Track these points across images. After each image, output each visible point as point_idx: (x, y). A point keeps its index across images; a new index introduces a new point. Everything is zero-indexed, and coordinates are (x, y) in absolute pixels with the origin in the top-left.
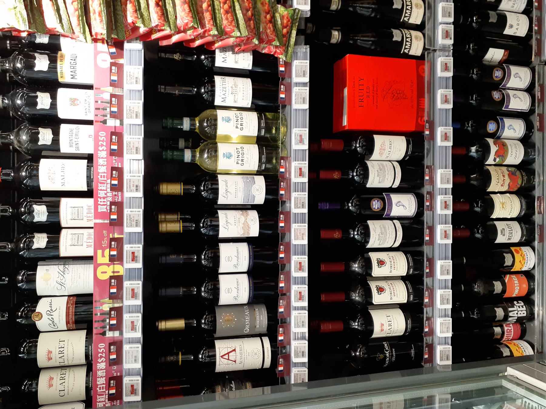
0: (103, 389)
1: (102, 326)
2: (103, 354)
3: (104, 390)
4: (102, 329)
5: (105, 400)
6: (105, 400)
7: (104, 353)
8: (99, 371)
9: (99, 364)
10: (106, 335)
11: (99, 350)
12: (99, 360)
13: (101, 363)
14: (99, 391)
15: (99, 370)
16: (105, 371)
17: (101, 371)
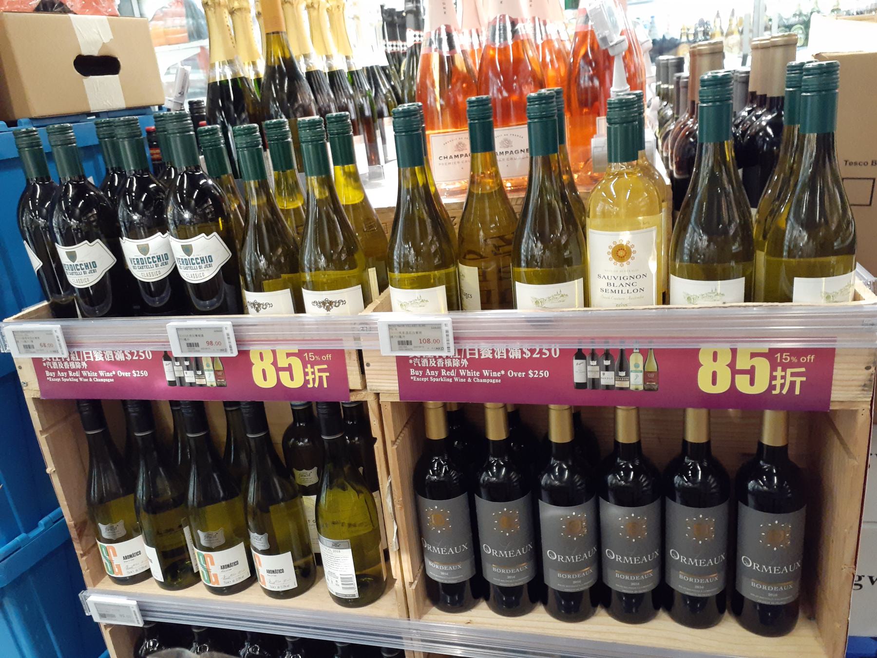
0: (470, 354)
3: (468, 357)
10: (576, 359)
16: (505, 357)
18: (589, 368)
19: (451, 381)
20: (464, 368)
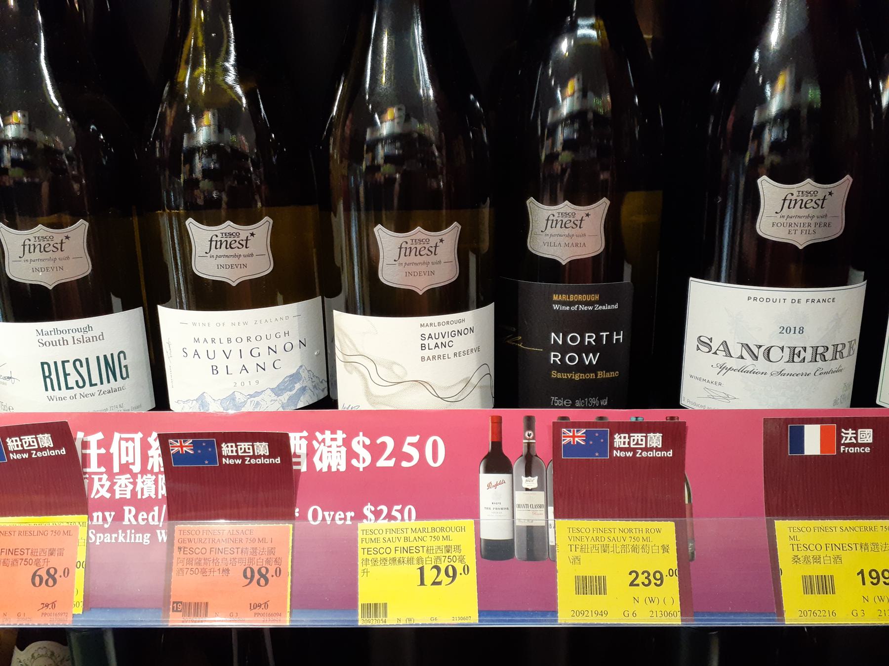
1: (537, 450)
2: (388, 458)
4: (524, 451)
5: (152, 472)
6: (152, 472)
7: (398, 463)
8: (304, 443)
10: (488, 470)
11: (415, 439)
12: (361, 438)
15: (310, 438)
18: (520, 497)
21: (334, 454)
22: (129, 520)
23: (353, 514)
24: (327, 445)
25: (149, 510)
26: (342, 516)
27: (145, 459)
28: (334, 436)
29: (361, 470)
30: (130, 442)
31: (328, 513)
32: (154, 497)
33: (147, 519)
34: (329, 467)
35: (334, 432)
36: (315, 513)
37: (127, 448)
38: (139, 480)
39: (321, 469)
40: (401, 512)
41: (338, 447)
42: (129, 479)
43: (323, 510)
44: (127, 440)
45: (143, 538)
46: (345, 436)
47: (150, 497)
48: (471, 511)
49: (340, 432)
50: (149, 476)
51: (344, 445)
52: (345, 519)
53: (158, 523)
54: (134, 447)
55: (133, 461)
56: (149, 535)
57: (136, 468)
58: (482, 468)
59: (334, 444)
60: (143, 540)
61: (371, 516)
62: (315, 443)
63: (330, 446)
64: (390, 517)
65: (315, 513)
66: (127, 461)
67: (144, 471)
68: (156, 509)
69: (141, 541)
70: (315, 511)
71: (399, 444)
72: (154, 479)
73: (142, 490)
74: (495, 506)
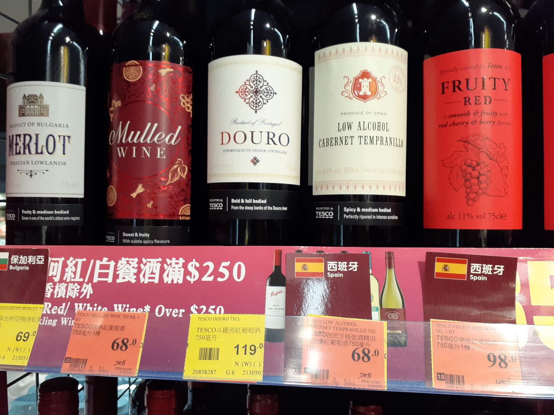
0: (101, 275)
2: (210, 276)
3: (96, 279)
5: (65, 282)
6: (65, 282)
7: (215, 279)
8: (159, 265)
9: (181, 265)
10: (272, 284)
11: (227, 264)
13: (182, 270)
14: (98, 263)
15: (163, 263)
16: (156, 281)
17: (157, 272)
19: (54, 324)
20: (84, 300)
21: (176, 272)
22: (46, 311)
23: (184, 311)
24: (172, 267)
25: (59, 305)
26: (177, 312)
27: (63, 273)
28: (177, 261)
29: (192, 283)
30: (56, 263)
31: (168, 309)
32: (64, 297)
33: (57, 311)
34: (172, 281)
35: (177, 259)
36: (160, 309)
37: (54, 266)
38: (57, 287)
39: (167, 282)
40: (215, 310)
41: (179, 268)
42: (51, 285)
43: (165, 308)
44: (55, 262)
45: (52, 322)
46: (184, 261)
47: (61, 297)
48: (260, 310)
49: (181, 259)
50: (63, 284)
51: (183, 267)
52: (179, 314)
53: (63, 313)
54: (58, 266)
55: (55, 275)
56: (56, 320)
57: (57, 279)
58: (268, 283)
59: (177, 266)
60: (52, 323)
61: (196, 312)
62: (165, 265)
63: (174, 268)
64: (207, 312)
65: (160, 309)
66: (52, 275)
67: (61, 281)
68: (64, 304)
69: (51, 324)
70: (160, 309)
71: (217, 267)
72: (65, 286)
73: (58, 292)
74: (275, 307)
